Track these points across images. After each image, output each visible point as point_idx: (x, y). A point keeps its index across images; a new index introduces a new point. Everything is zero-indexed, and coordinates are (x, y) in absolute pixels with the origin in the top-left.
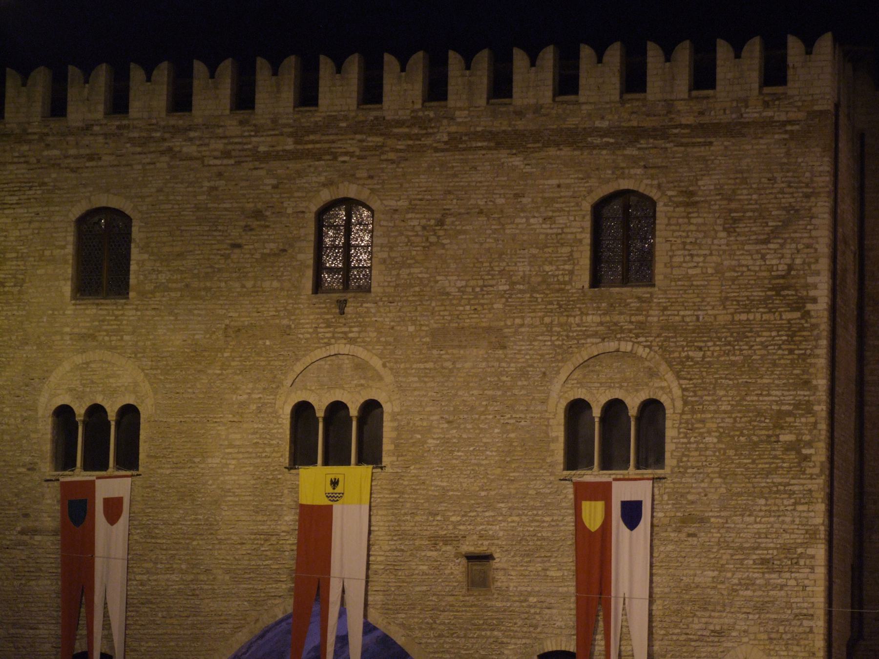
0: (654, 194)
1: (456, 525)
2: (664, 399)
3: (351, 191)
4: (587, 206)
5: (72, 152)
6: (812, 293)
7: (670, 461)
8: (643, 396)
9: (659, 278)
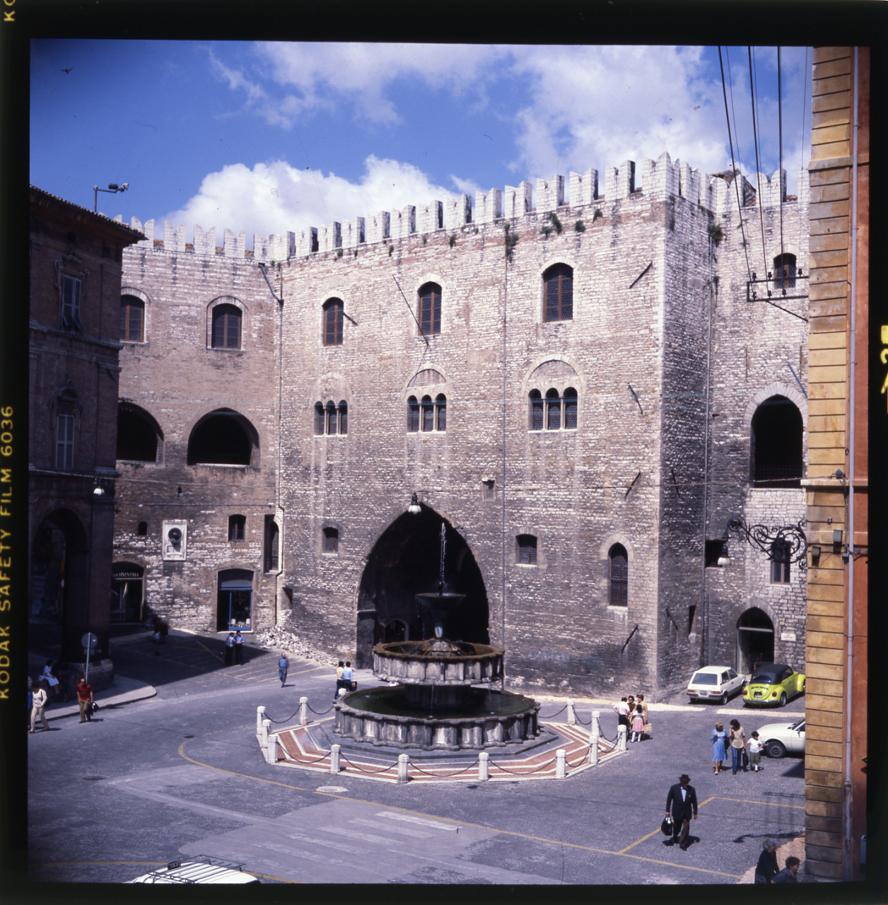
0: (572, 265)
1: (479, 462)
2: (576, 387)
3: (434, 278)
4: (539, 275)
5: (322, 269)
6: (655, 317)
7: (579, 424)
8: (567, 386)
9: (574, 314)
